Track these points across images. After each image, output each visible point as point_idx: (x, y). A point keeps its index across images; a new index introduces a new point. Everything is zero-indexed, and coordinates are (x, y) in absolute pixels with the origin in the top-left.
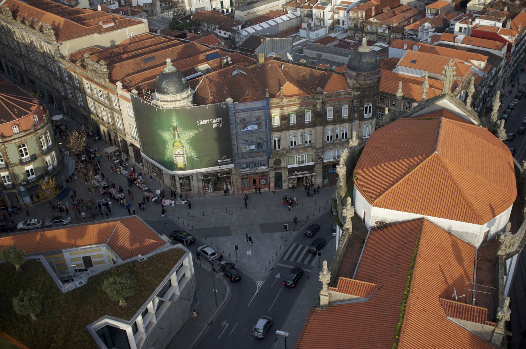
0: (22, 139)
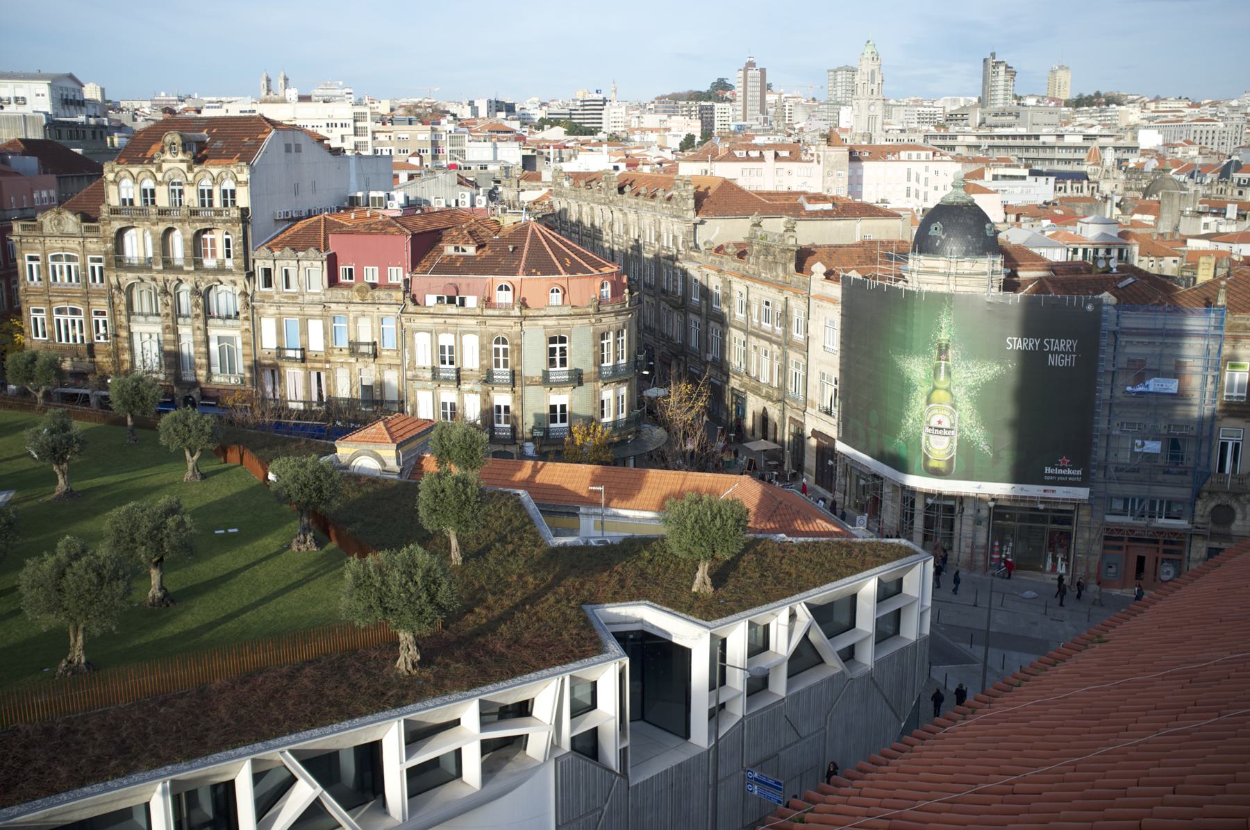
0: (562, 322)
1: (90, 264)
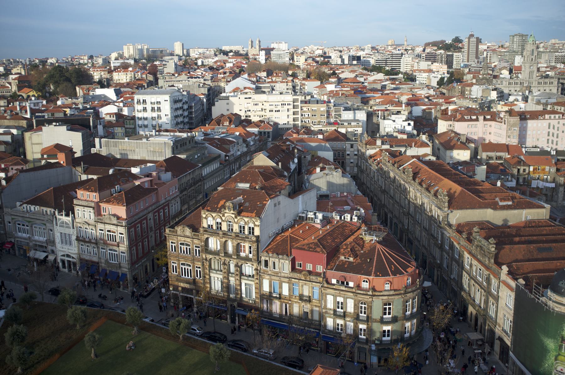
1: (195, 248)
